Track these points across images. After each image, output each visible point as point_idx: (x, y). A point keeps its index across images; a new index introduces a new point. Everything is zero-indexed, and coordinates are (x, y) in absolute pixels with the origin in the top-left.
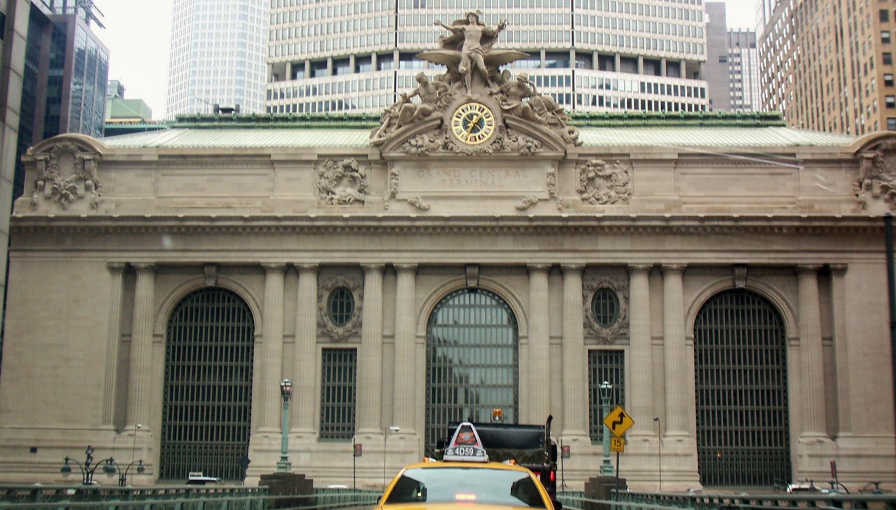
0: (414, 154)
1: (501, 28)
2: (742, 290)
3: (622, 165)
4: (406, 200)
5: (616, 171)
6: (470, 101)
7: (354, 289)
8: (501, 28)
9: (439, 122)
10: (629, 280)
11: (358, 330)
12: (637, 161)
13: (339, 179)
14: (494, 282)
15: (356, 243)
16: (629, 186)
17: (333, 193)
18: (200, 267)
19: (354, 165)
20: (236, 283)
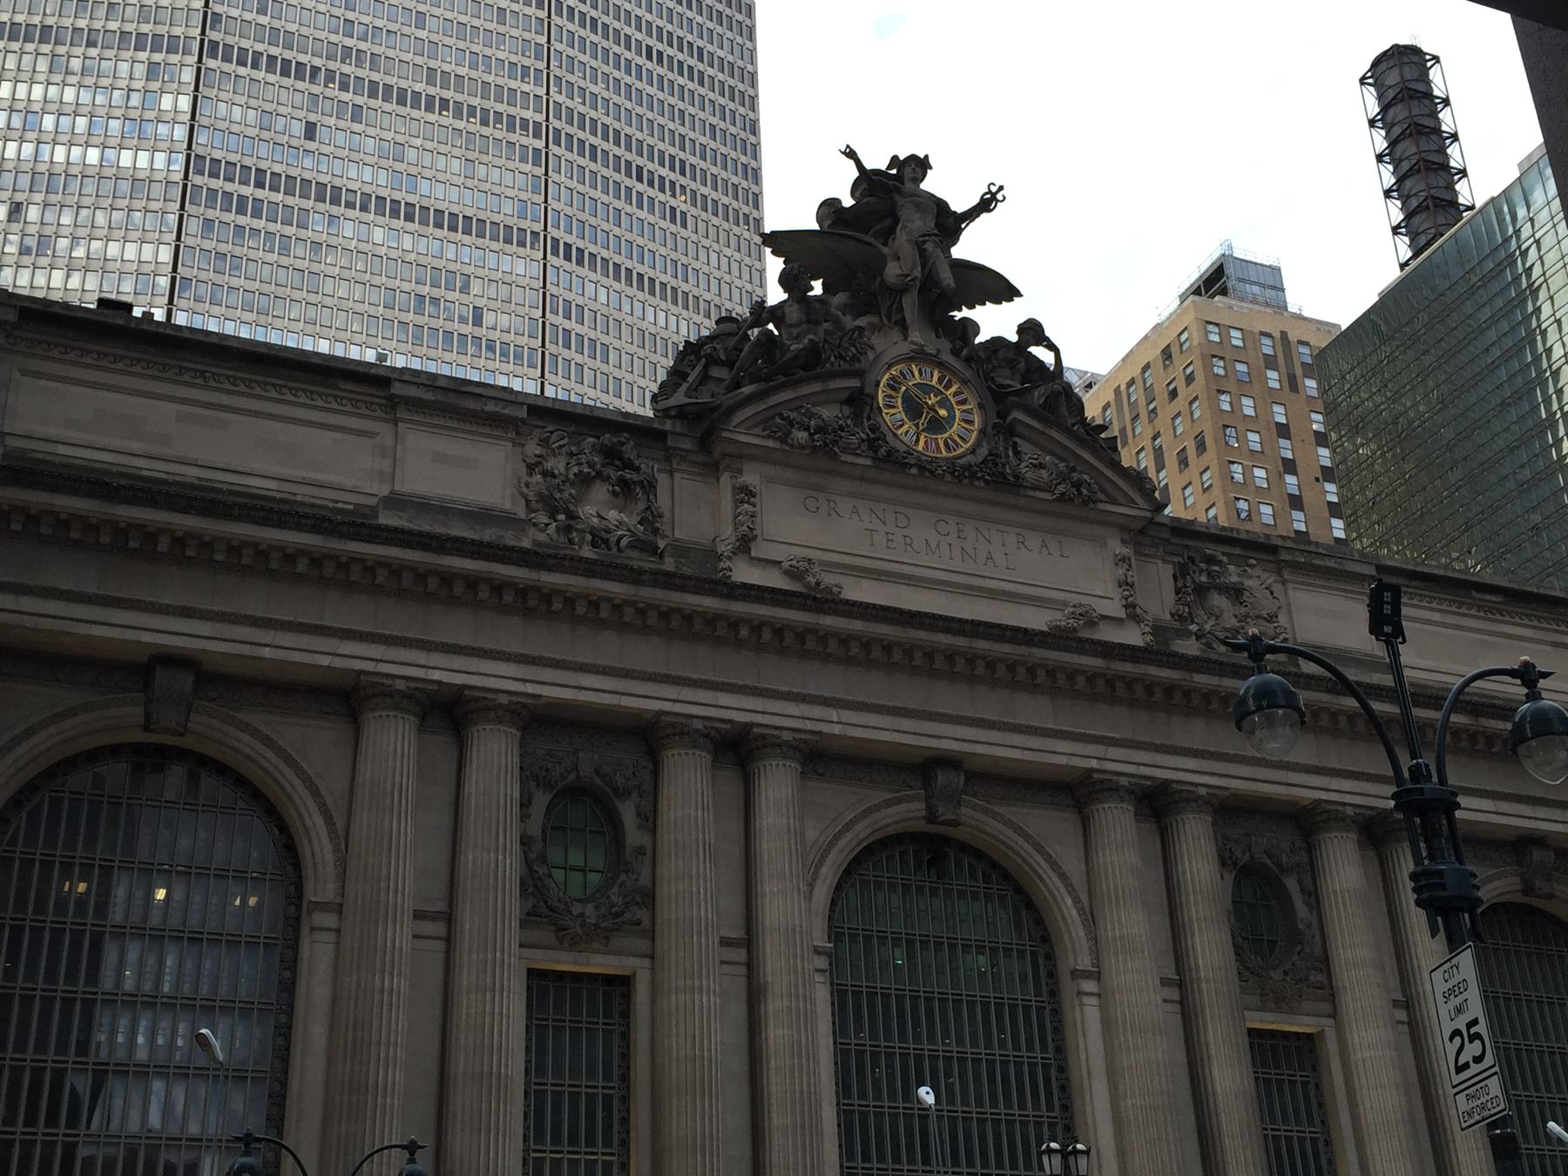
0: (802, 447)
1: (987, 203)
2: (1532, 910)
3: (1257, 572)
5: (1248, 583)
6: (919, 356)
7: (623, 794)
8: (987, 203)
9: (854, 383)
10: (1311, 849)
11: (643, 915)
13: (585, 481)
14: (995, 816)
15: (644, 653)
16: (1283, 619)
17: (572, 516)
18: (144, 671)
19: (629, 451)
20: (255, 733)
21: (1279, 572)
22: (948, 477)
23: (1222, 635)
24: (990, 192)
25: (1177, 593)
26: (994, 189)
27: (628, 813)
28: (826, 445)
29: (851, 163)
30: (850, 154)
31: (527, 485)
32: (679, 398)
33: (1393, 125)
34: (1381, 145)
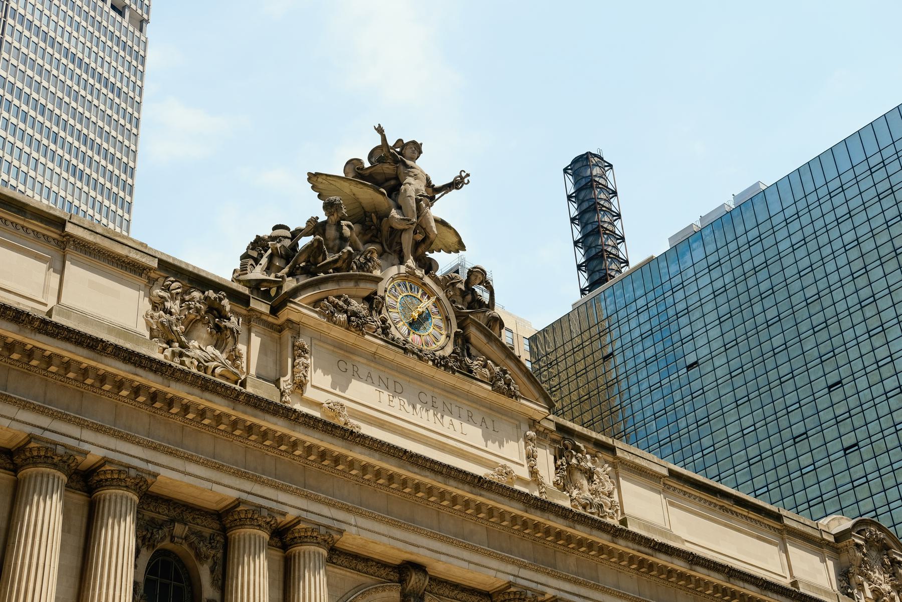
1: (456, 184)
4: (319, 405)
8: (456, 184)
12: (622, 462)
17: (183, 345)
21: (614, 466)
22: (430, 363)
23: (583, 502)
24: (460, 176)
25: (556, 469)
26: (463, 174)
27: (205, 574)
28: (358, 325)
29: (379, 136)
30: (380, 130)
31: (152, 317)
32: (257, 273)
33: (583, 201)
34: (574, 213)
